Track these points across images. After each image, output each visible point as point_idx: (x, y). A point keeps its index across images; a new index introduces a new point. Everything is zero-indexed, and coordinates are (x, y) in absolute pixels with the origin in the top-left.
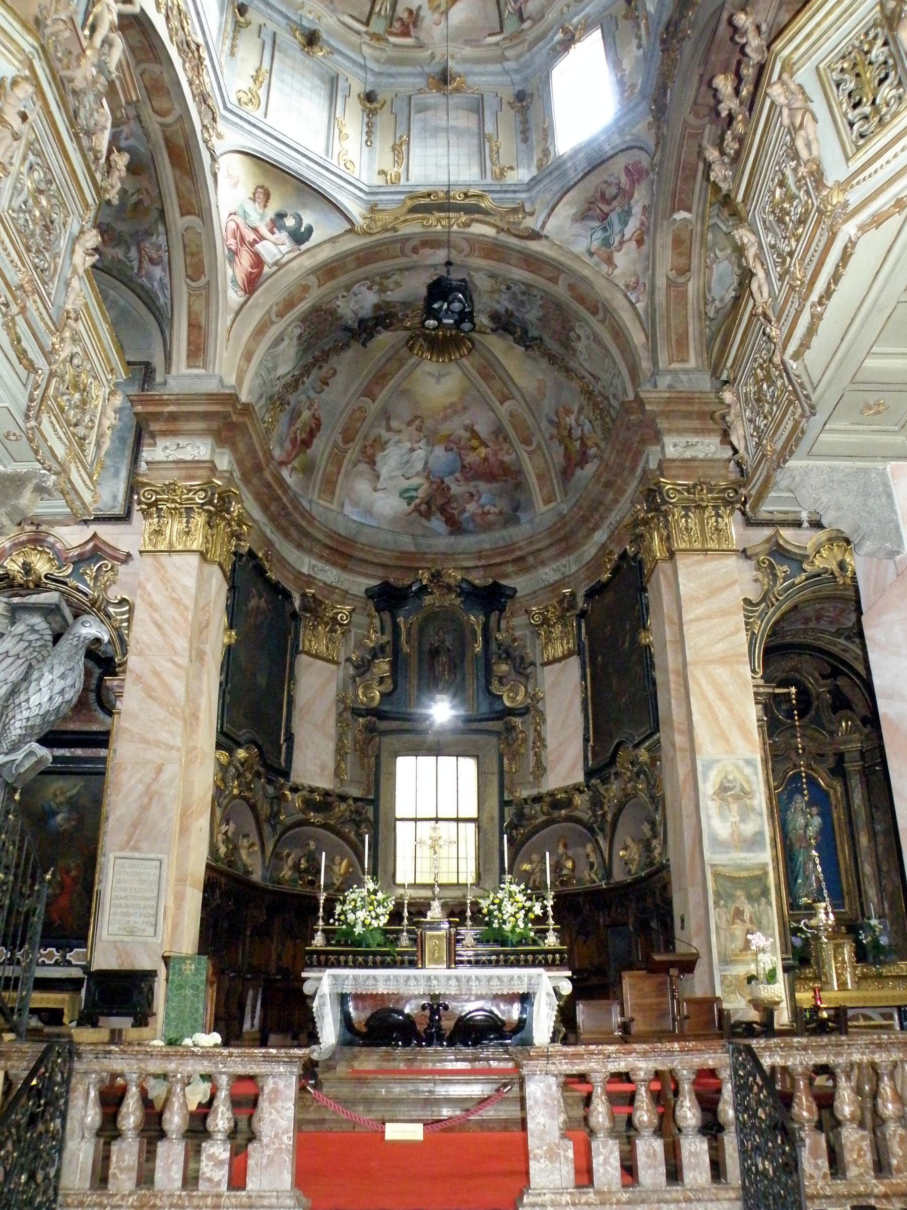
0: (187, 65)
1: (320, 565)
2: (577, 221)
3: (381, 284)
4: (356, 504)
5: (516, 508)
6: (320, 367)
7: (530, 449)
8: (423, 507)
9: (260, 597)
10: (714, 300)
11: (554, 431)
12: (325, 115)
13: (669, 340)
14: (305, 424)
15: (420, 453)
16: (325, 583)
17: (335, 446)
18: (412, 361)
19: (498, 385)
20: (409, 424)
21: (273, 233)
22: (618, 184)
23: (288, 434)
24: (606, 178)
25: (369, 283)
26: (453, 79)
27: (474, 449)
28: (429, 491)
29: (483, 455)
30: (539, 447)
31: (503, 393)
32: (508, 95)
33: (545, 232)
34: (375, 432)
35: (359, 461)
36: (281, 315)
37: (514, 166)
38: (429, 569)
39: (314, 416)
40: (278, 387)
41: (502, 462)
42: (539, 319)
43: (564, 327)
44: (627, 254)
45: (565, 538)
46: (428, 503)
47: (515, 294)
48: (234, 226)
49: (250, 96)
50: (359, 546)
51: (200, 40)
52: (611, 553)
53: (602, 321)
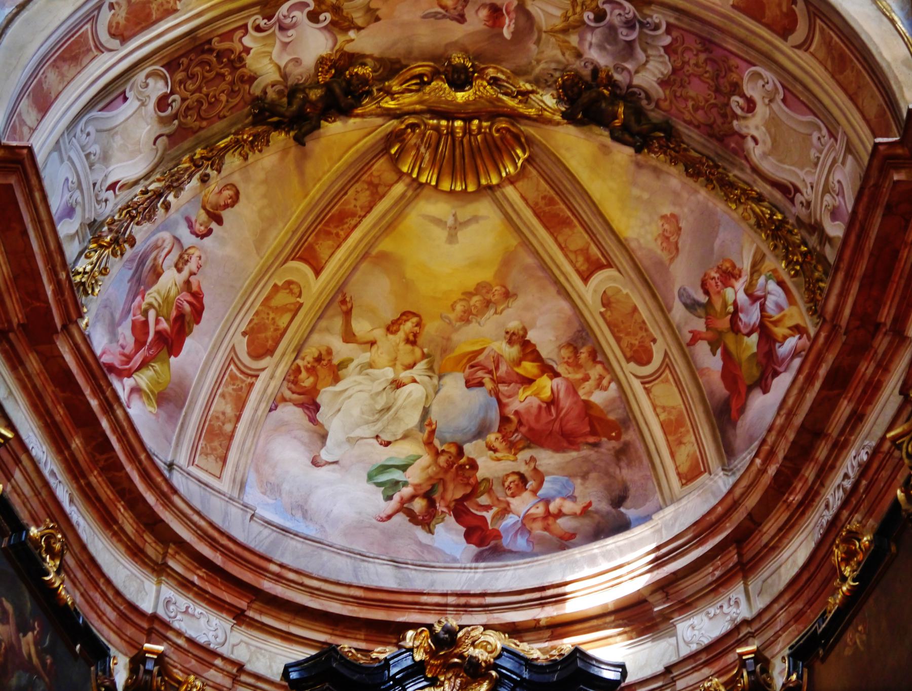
1: (182, 601)
4: (272, 488)
5: (619, 501)
6: (204, 179)
8: (419, 505)
9: (23, 628)
11: (699, 325)
14: (166, 299)
15: (414, 393)
16: (190, 640)
17: (232, 359)
18: (399, 188)
19: (578, 238)
20: (392, 328)
27: (528, 381)
28: (432, 470)
29: (546, 394)
30: (667, 364)
35: (284, 400)
36: (121, 35)
38: (430, 627)
39: (188, 283)
41: (587, 405)
43: (717, 90)
45: (739, 539)
46: (428, 496)
47: (612, 28)
50: (274, 568)
52: (854, 536)
53: (804, 46)
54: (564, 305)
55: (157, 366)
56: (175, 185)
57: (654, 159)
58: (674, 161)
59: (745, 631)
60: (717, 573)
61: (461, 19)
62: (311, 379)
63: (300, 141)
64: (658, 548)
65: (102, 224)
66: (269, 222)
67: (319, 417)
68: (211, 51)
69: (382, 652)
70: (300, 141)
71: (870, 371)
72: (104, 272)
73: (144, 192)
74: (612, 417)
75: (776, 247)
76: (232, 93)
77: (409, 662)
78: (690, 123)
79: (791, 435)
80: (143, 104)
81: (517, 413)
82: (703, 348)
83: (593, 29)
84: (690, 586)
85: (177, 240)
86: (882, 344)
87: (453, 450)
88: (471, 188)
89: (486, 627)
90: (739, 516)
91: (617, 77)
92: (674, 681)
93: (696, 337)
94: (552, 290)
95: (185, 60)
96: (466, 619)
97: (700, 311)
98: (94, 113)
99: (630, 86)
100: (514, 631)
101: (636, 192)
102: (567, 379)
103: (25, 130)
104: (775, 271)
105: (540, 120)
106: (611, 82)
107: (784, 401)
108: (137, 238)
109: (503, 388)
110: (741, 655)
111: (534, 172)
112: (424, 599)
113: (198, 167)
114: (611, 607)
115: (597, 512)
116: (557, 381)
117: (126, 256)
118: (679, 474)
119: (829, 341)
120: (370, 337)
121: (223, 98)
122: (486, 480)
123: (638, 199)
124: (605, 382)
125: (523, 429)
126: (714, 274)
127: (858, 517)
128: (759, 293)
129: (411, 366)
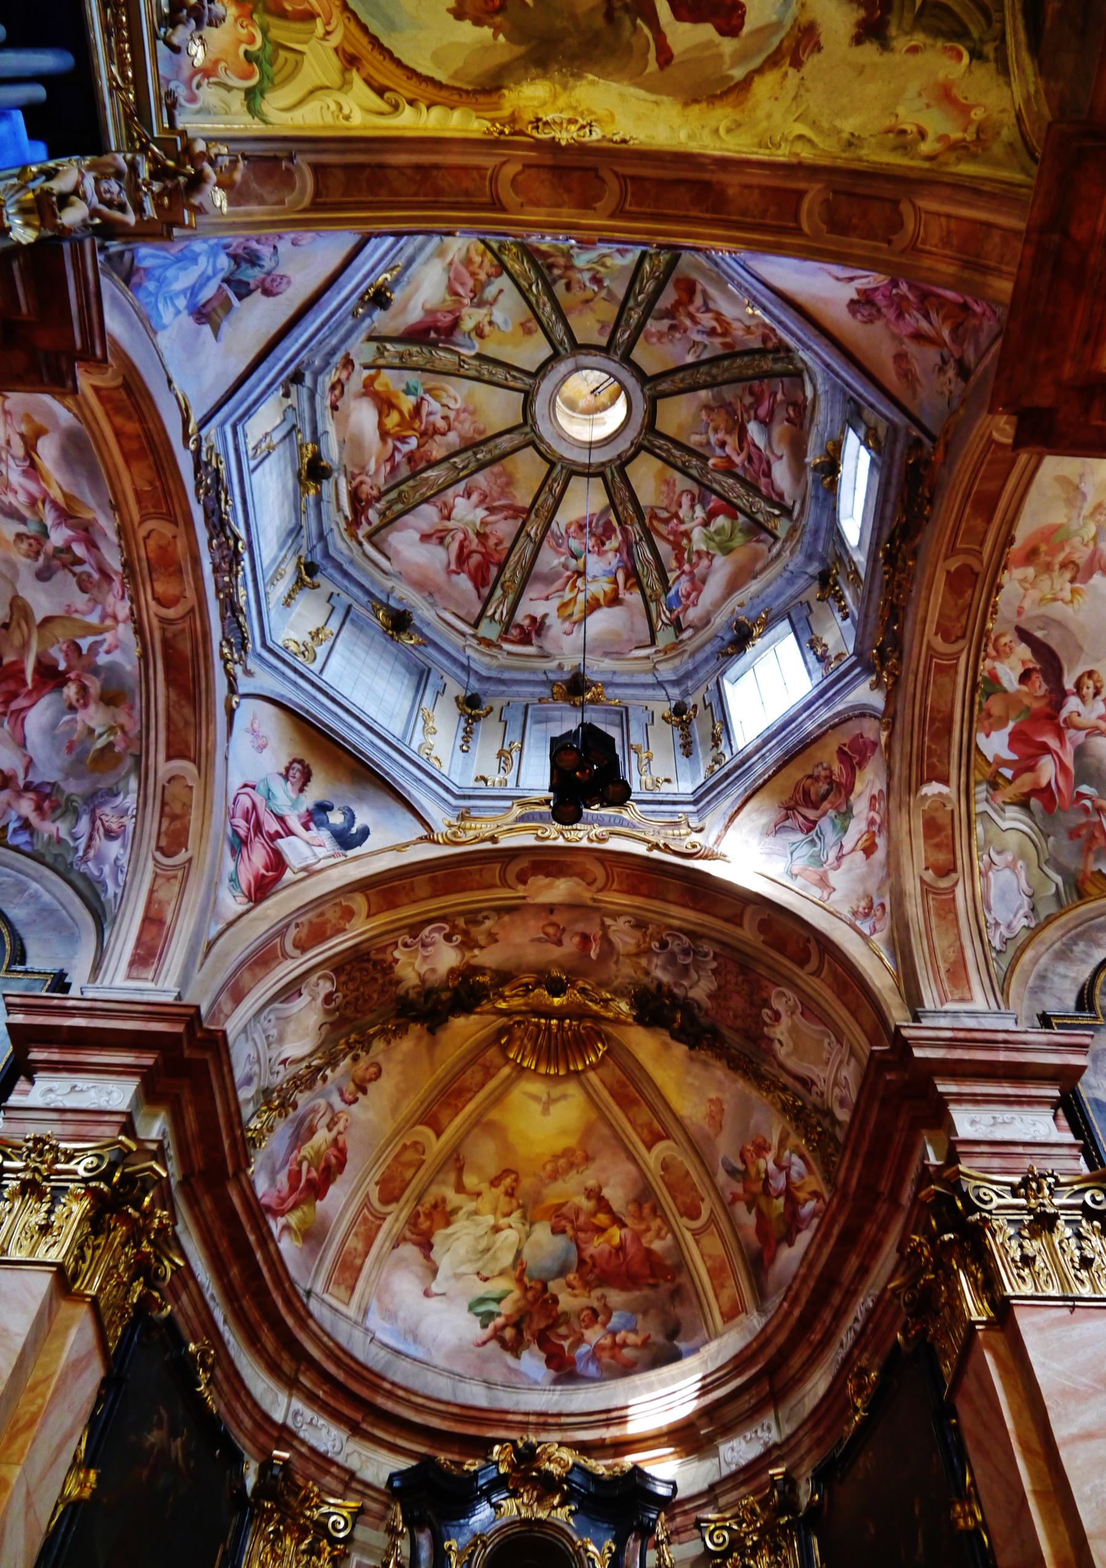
0: (215, 542)
2: (768, 835)
3: (466, 933)
4: (390, 1315)
6: (356, 1059)
7: (696, 1224)
8: (509, 1333)
10: (997, 924)
11: (739, 1188)
12: (407, 705)
13: (936, 971)
14: (318, 1153)
15: (510, 1237)
17: (366, 1203)
18: (506, 1071)
19: (644, 1115)
20: (494, 1183)
21: (308, 829)
22: (829, 778)
23: (285, 1162)
24: (809, 772)
25: (447, 928)
26: (588, 689)
27: (601, 1230)
28: (522, 1303)
29: (616, 1241)
30: (712, 1220)
31: (651, 1131)
32: (663, 708)
33: (721, 849)
34: (436, 1191)
35: (405, 1239)
36: (302, 947)
37: (673, 778)
38: (514, 1443)
40: (281, 1077)
41: (649, 1252)
42: (711, 996)
43: (752, 1004)
44: (850, 870)
45: (771, 1371)
48: (249, 804)
49: (302, 649)
50: (387, 1385)
51: (241, 532)
52: (865, 1371)
53: (817, 973)
54: (631, 1168)
55: (305, 1208)
56: (332, 1062)
57: (703, 1055)
58: (719, 1057)
59: (776, 1453)
60: (753, 1401)
61: (559, 943)
62: (428, 1223)
63: (432, 1031)
64: (704, 1378)
65: (273, 1092)
66: (403, 1094)
67: (433, 1255)
68: (369, 960)
69: (472, 1465)
70: (432, 1031)
71: (872, 1233)
72: (271, 1129)
73: (308, 1067)
74: (669, 1262)
75: (797, 1127)
76: (382, 992)
77: (494, 1475)
78: (731, 1028)
79: (812, 1283)
80: (314, 999)
81: (592, 1256)
82: (741, 1208)
83: (658, 954)
84: (731, 1411)
85: (330, 1106)
86: (882, 1209)
87: (539, 1286)
88: (562, 1073)
89: (561, 1444)
90: (771, 1350)
91: (676, 990)
92: (716, 1498)
93: (735, 1198)
94: (623, 1156)
95: (348, 967)
96: (544, 1437)
97: (739, 1177)
98: (276, 1005)
99: (686, 997)
100: (584, 1448)
101: (689, 1080)
102: (632, 1230)
103: (222, 1016)
104: (797, 1147)
105: (617, 1021)
106: (672, 995)
107: (806, 1253)
108: (300, 1103)
109: (581, 1235)
110: (773, 1476)
111: (611, 1062)
112: (510, 1417)
113: (351, 1047)
114: (665, 1430)
115: (655, 1344)
116: (625, 1231)
117: (290, 1117)
118: (722, 1313)
119: (840, 1206)
120: (477, 1189)
121: (375, 996)
122: (565, 1313)
123: (691, 1085)
124: (663, 1233)
125: (597, 1271)
126: (750, 1147)
127: (866, 1355)
128: (784, 1164)
129: (508, 1215)
